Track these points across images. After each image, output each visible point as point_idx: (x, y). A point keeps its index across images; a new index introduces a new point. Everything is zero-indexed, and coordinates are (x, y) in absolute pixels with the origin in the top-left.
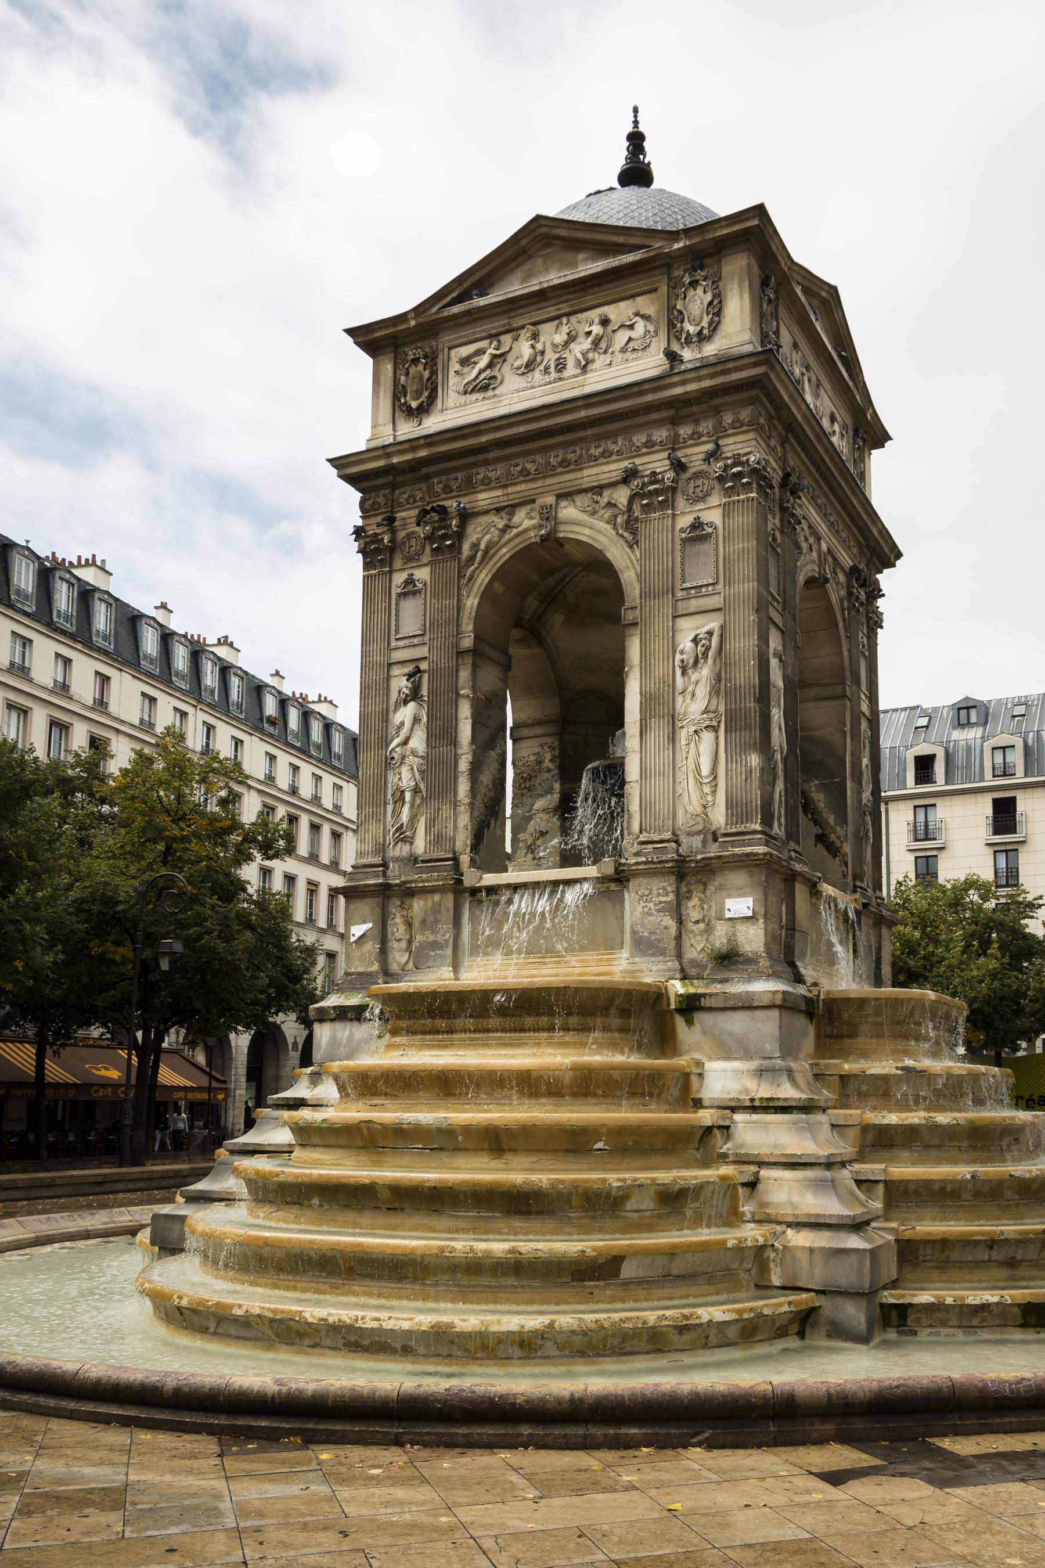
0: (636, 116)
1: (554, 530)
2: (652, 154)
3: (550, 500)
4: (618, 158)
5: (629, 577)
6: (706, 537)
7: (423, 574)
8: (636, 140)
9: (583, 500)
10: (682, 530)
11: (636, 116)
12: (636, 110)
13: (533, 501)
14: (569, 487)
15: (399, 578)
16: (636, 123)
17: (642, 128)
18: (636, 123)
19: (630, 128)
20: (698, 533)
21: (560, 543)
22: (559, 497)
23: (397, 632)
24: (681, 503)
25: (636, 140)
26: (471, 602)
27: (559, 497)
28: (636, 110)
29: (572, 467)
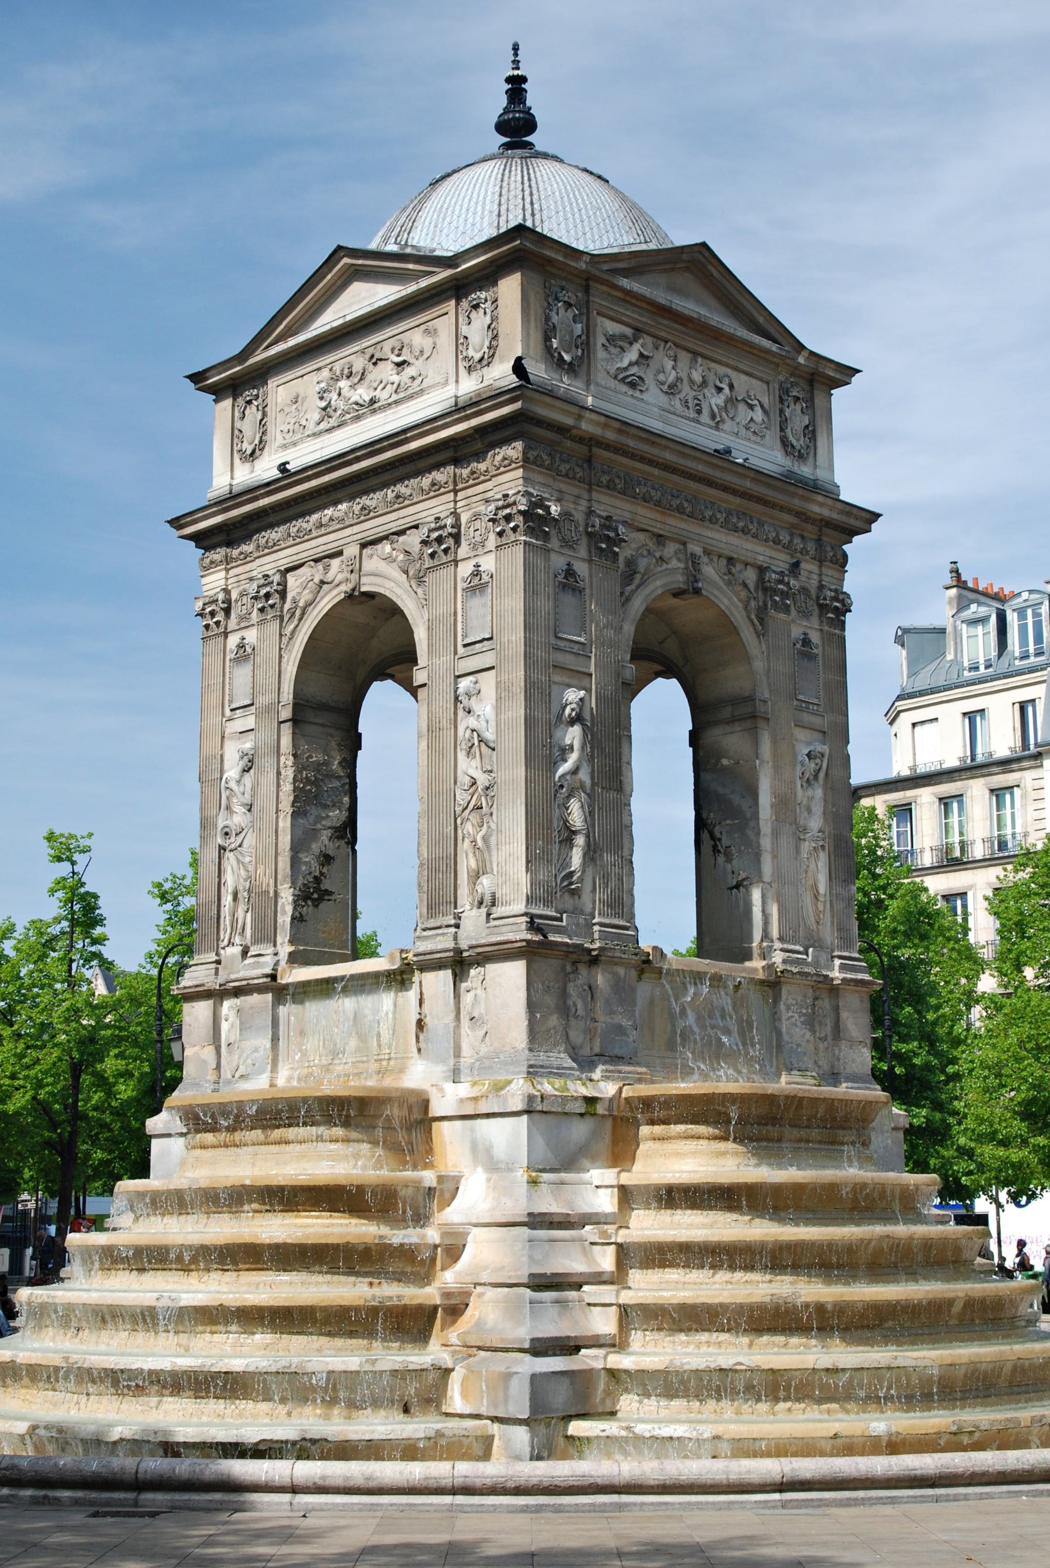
1: (359, 584)
5: (420, 635)
6: (482, 588)
7: (251, 636)
8: (516, 86)
9: (386, 548)
12: (516, 48)
13: (340, 553)
14: (370, 535)
15: (233, 641)
20: (477, 584)
21: (371, 596)
22: (363, 546)
23: (231, 702)
24: (463, 551)
25: (516, 86)
26: (291, 669)
28: (516, 48)
29: (372, 514)
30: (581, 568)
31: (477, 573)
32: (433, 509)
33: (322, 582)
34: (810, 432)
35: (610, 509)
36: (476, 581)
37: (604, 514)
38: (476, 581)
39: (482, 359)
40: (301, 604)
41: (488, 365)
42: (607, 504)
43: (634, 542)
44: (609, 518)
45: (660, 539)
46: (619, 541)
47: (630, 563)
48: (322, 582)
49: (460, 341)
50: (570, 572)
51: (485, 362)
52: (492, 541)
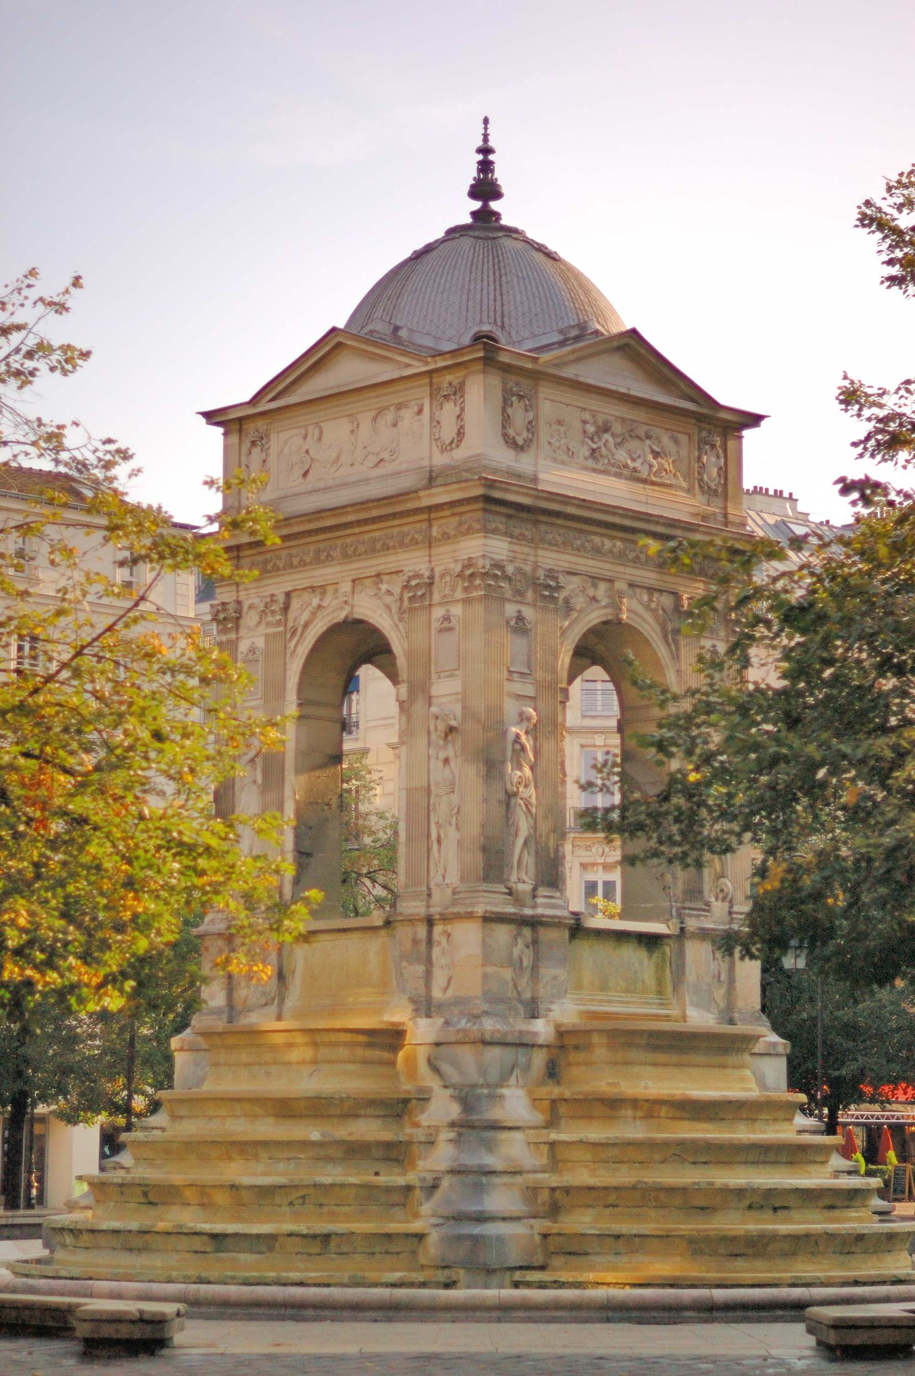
0: (486, 129)
2: (501, 175)
3: (346, 587)
6: (451, 629)
10: (437, 620)
11: (486, 129)
12: (486, 121)
17: (491, 143)
19: (479, 143)
27: (354, 581)
28: (486, 121)
30: (528, 613)
31: (447, 618)
32: (414, 562)
34: (724, 472)
35: (552, 562)
37: (548, 567)
38: (446, 625)
39: (452, 441)
40: (302, 622)
41: (458, 446)
42: (550, 559)
43: (571, 585)
44: (550, 570)
45: (595, 579)
46: (559, 588)
47: (567, 601)
49: (436, 423)
50: (520, 618)
51: (454, 445)
52: (459, 594)
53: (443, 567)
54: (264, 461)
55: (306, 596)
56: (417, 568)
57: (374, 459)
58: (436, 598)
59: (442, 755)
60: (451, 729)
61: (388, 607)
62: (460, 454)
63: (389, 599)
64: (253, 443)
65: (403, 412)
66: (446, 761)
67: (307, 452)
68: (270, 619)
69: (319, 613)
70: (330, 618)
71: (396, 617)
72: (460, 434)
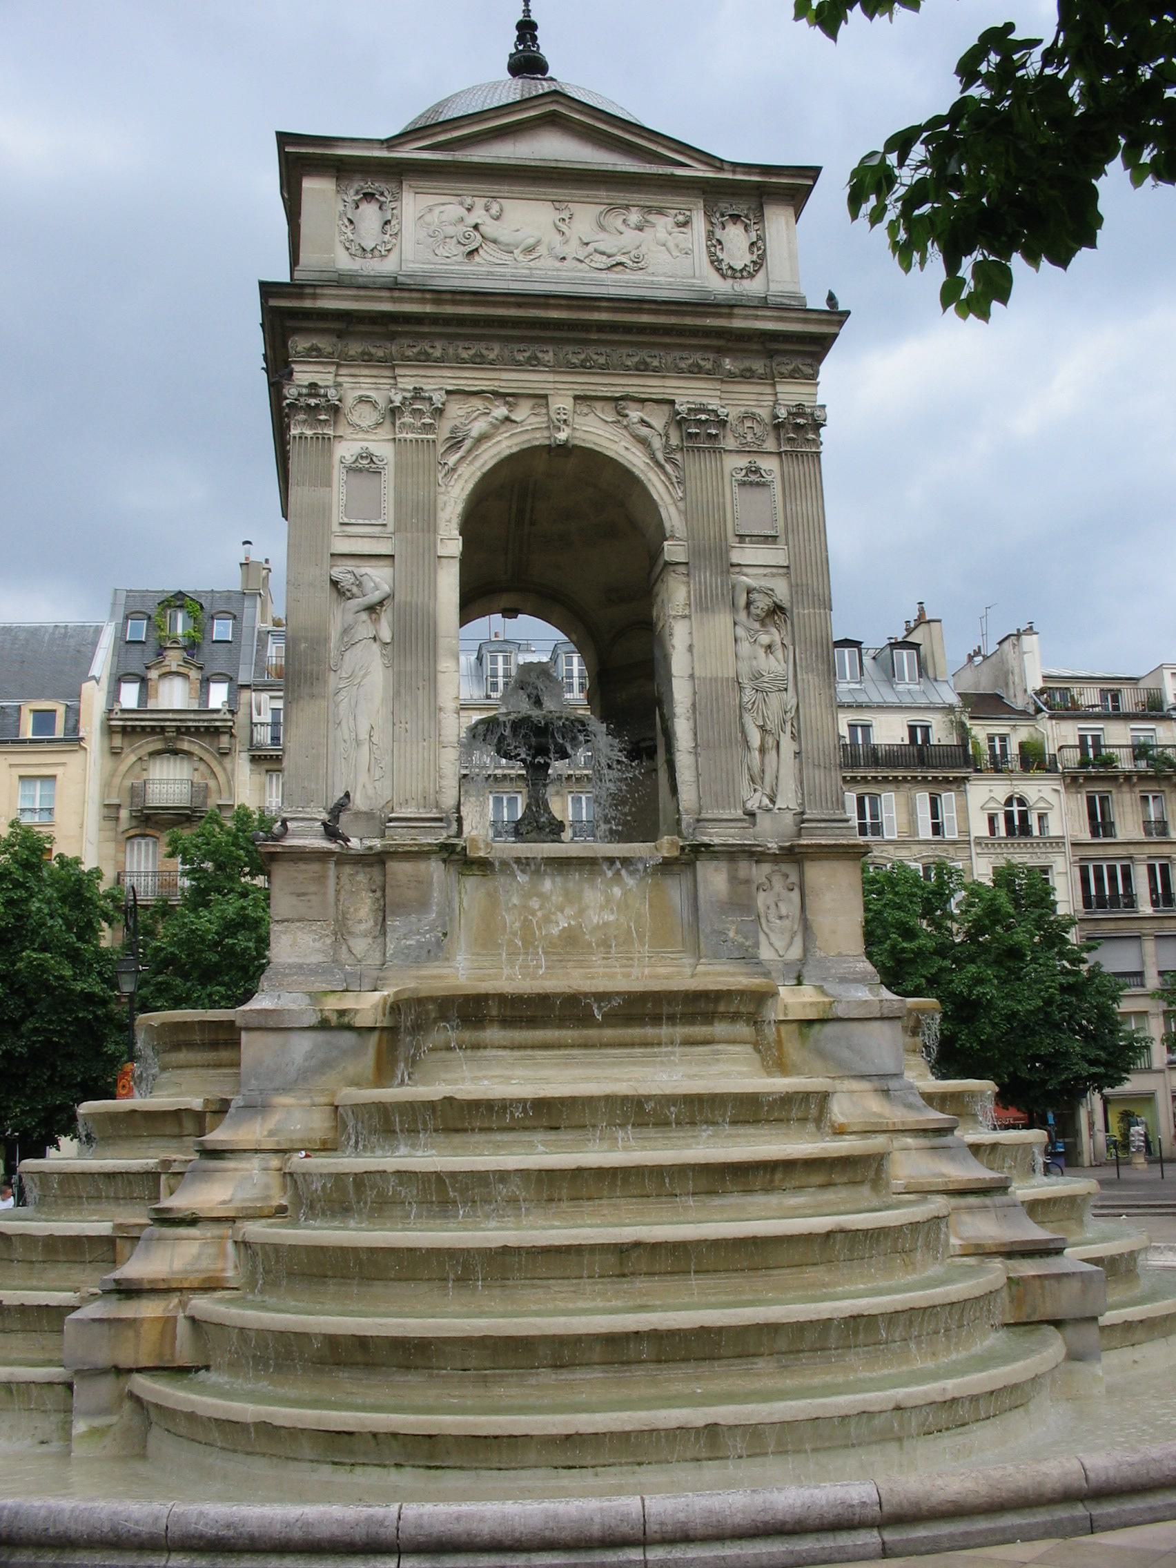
4: (508, 43)
8: (527, 29)
16: (527, 11)
18: (527, 11)
19: (520, 17)
25: (527, 29)
32: (691, 393)
33: (507, 419)
36: (753, 478)
38: (753, 478)
40: (475, 433)
41: (752, 276)
48: (507, 419)
53: (743, 409)
54: (387, 222)
55: (478, 403)
56: (705, 401)
57: (603, 261)
58: (730, 443)
59: (765, 639)
60: (777, 610)
61: (644, 442)
62: (753, 287)
63: (644, 431)
64: (368, 197)
65: (652, 218)
66: (769, 648)
67: (476, 227)
68: (407, 419)
69: (503, 429)
70: (526, 437)
71: (660, 456)
72: (759, 263)
